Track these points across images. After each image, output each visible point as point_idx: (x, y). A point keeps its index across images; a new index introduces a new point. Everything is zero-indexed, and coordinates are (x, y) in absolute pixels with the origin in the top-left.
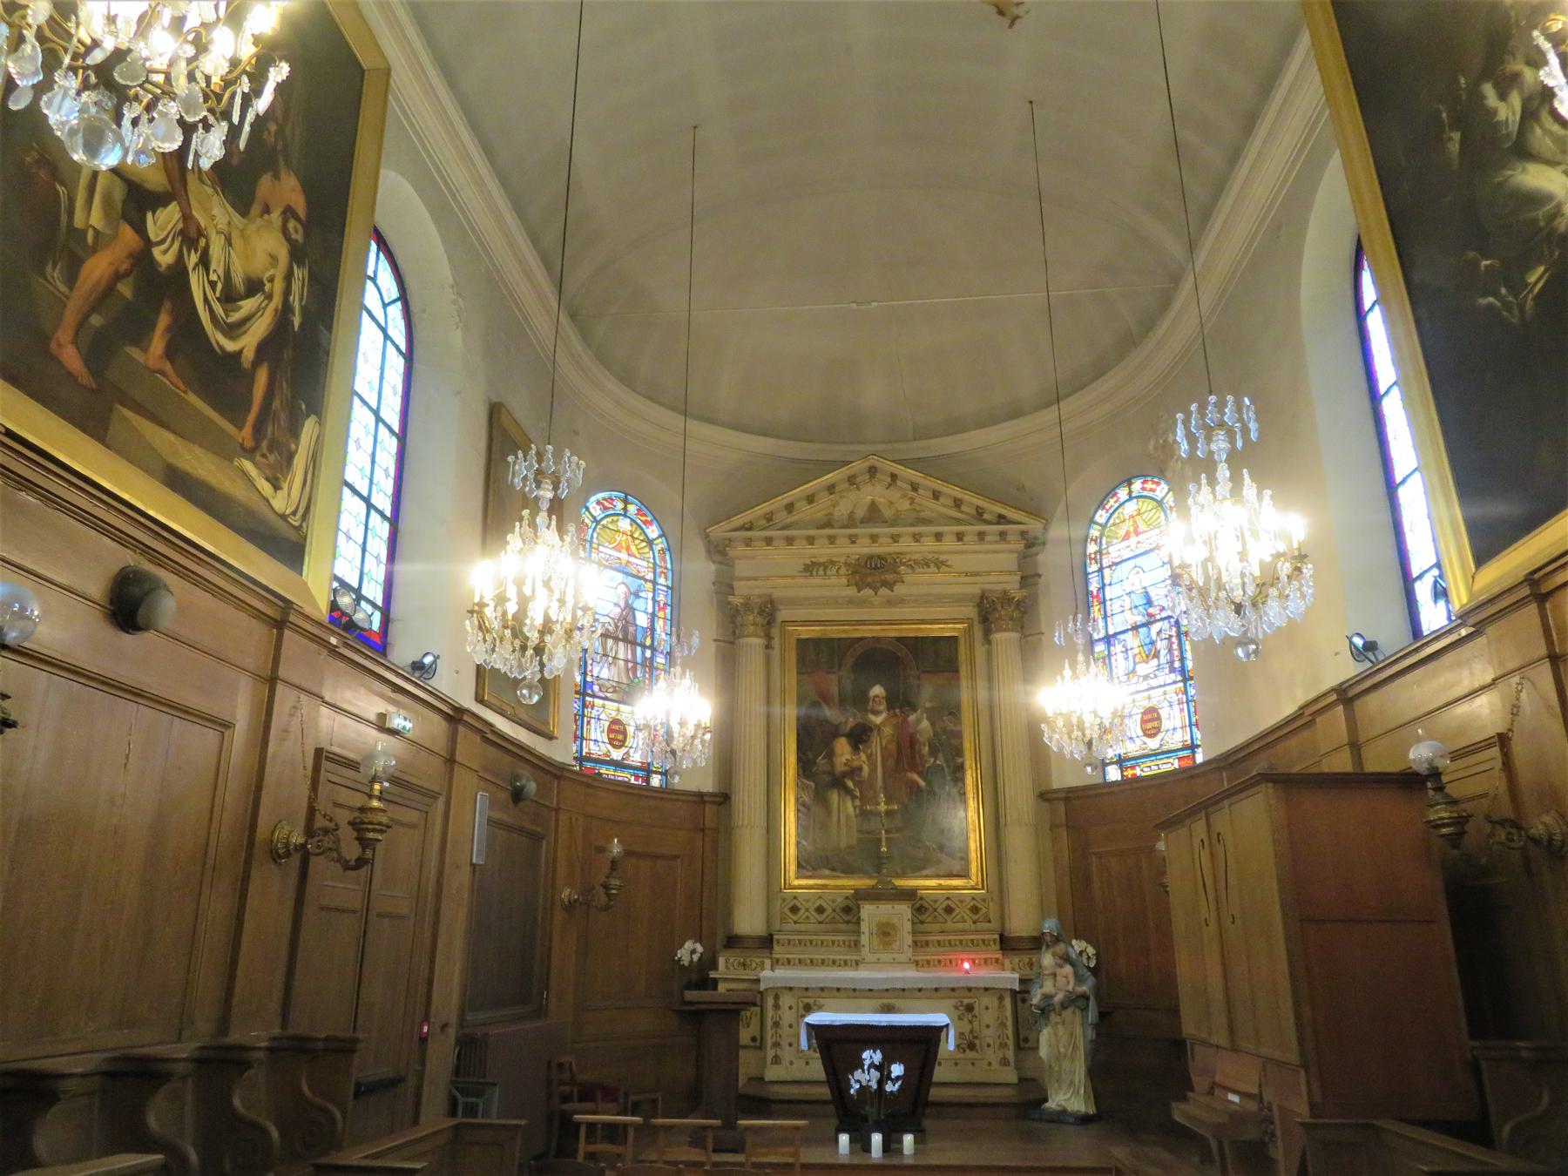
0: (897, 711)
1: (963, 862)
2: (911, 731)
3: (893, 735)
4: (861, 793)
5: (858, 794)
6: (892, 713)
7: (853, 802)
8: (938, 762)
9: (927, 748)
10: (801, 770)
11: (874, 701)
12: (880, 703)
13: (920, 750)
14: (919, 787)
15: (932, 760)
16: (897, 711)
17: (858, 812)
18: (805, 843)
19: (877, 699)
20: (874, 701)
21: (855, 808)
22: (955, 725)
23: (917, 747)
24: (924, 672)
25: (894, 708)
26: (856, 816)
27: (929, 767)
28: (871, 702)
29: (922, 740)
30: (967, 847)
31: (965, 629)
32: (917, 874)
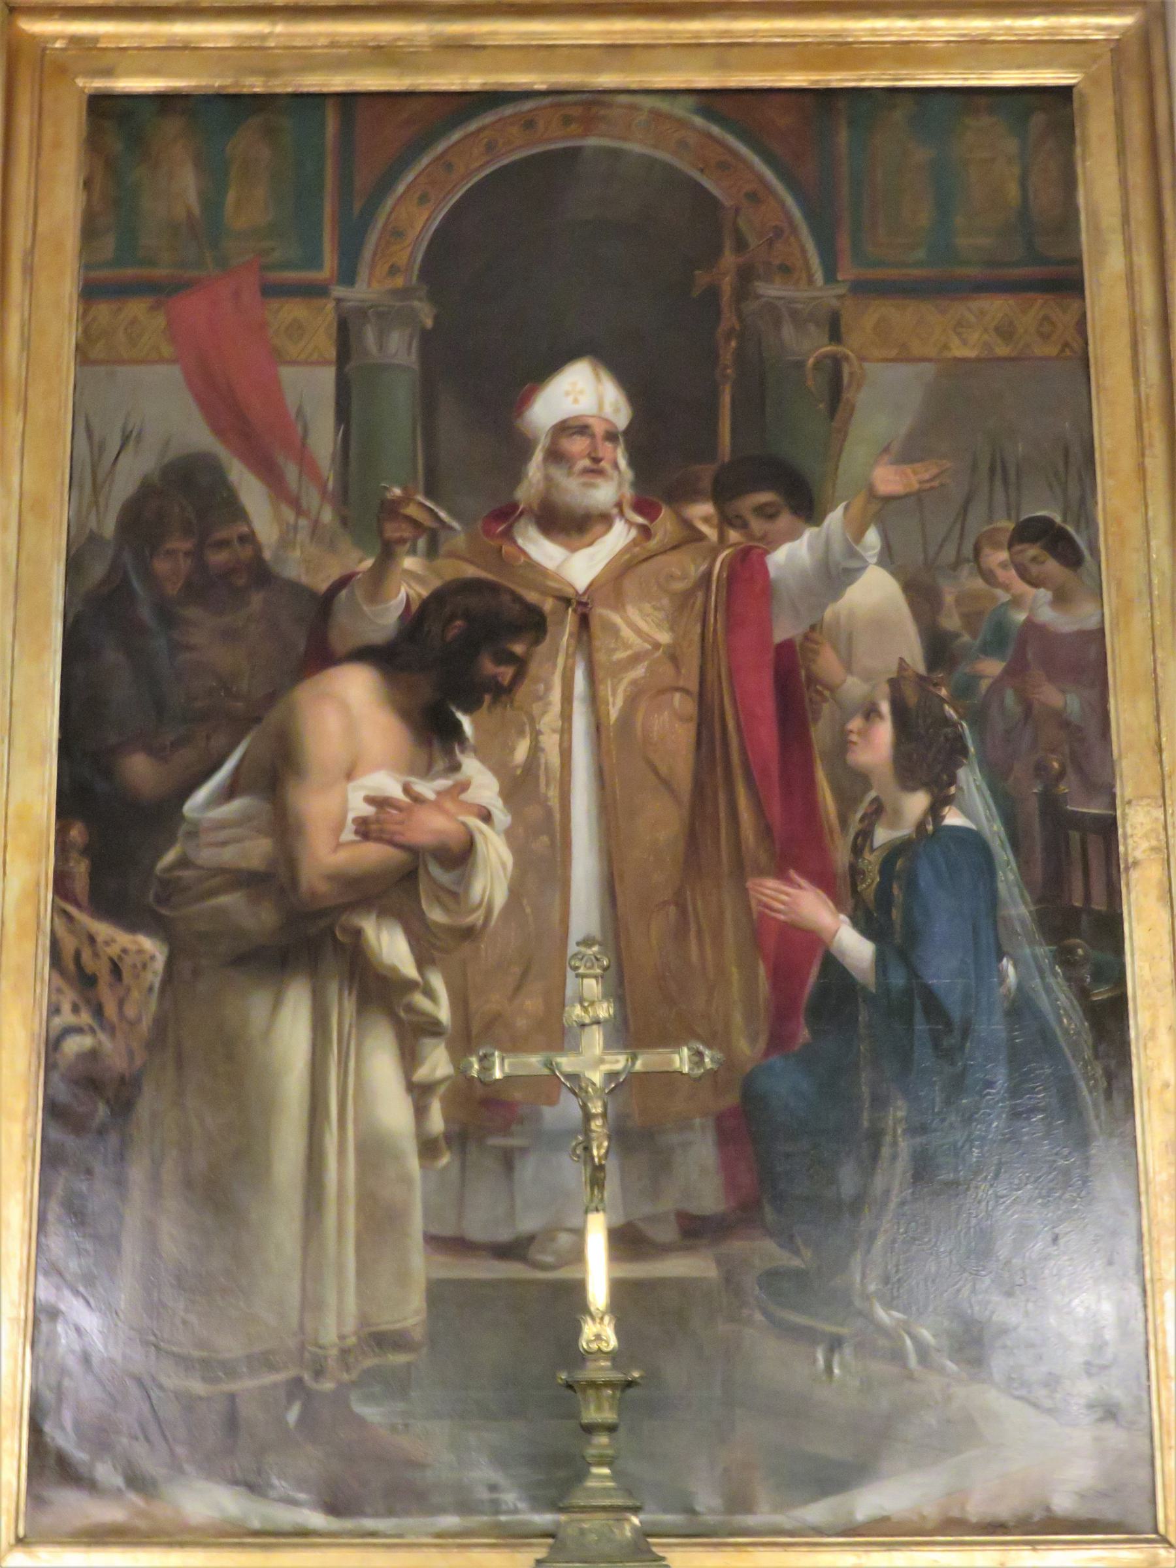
0: (701, 511)
1: (1115, 1436)
2: (784, 630)
3: (673, 657)
4: (460, 1001)
5: (444, 1013)
6: (665, 525)
7: (409, 1058)
8: (953, 818)
9: (884, 732)
10: (81, 868)
11: (555, 455)
12: (595, 471)
13: (843, 744)
14: (832, 965)
15: (917, 803)
16: (701, 511)
17: (437, 1122)
18: (91, 1322)
19: (577, 445)
20: (555, 455)
21: (419, 1093)
22: (1061, 598)
23: (820, 734)
24: (863, 289)
25: (680, 494)
26: (428, 1148)
27: (897, 850)
28: (535, 469)
29: (854, 687)
30: (941, 1175)
31: (1117, 48)
32: (816, 1512)
